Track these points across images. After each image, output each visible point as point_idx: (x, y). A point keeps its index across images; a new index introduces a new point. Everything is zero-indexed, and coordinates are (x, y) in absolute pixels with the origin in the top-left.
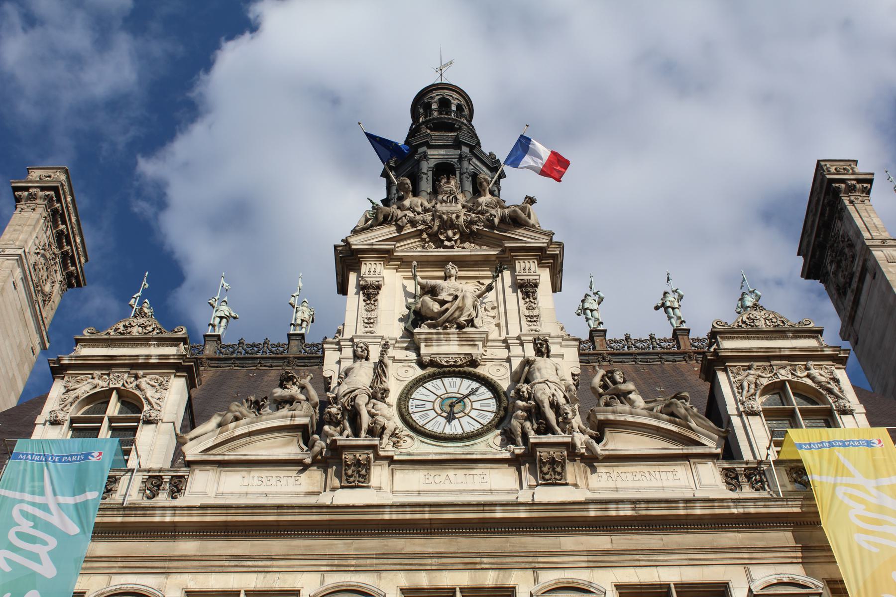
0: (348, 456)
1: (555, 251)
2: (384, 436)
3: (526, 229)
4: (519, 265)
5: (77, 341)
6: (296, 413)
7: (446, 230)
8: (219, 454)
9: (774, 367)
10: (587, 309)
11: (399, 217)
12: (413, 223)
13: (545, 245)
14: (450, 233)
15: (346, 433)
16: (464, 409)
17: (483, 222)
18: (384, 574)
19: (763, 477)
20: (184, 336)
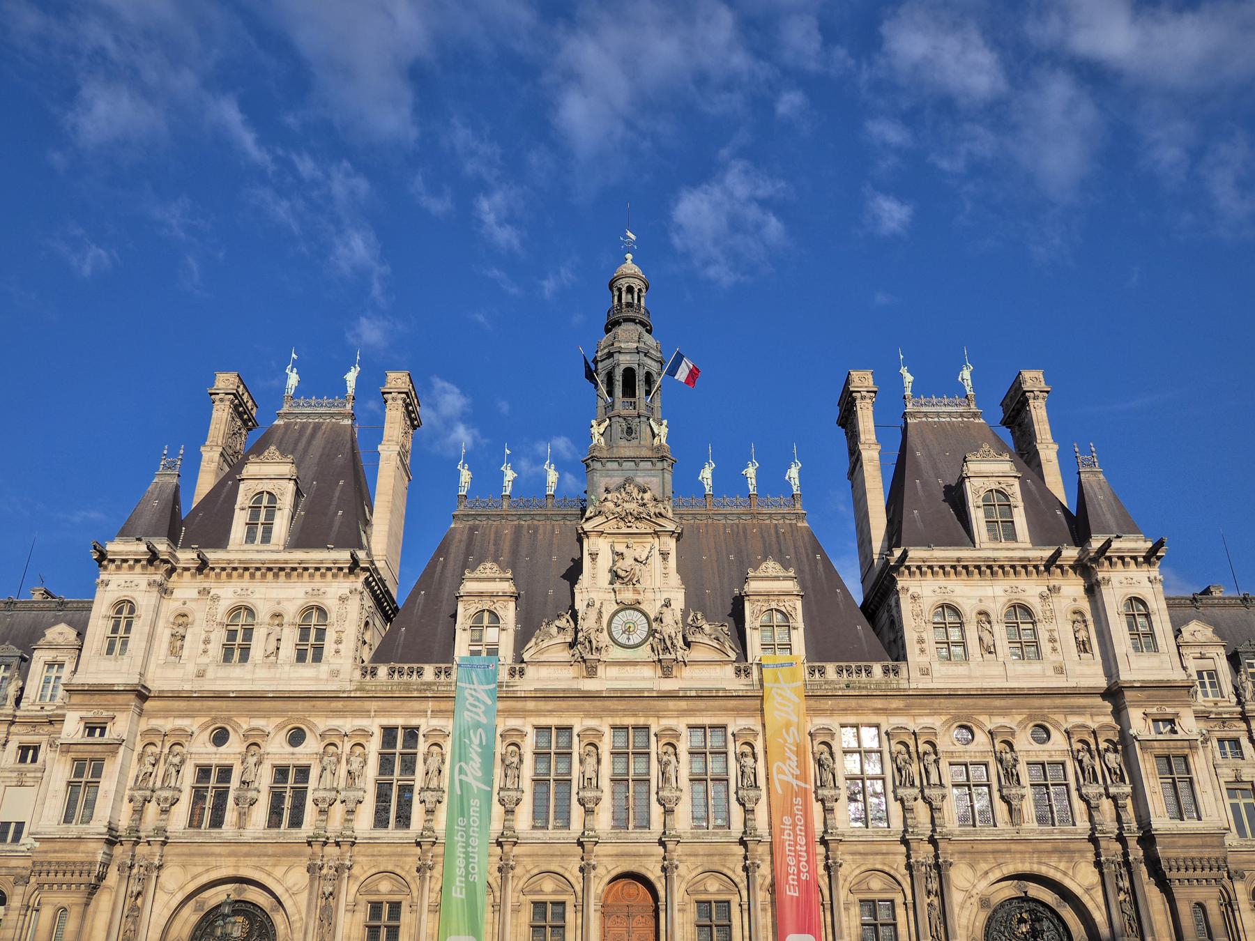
4: (662, 539)
12: (613, 514)
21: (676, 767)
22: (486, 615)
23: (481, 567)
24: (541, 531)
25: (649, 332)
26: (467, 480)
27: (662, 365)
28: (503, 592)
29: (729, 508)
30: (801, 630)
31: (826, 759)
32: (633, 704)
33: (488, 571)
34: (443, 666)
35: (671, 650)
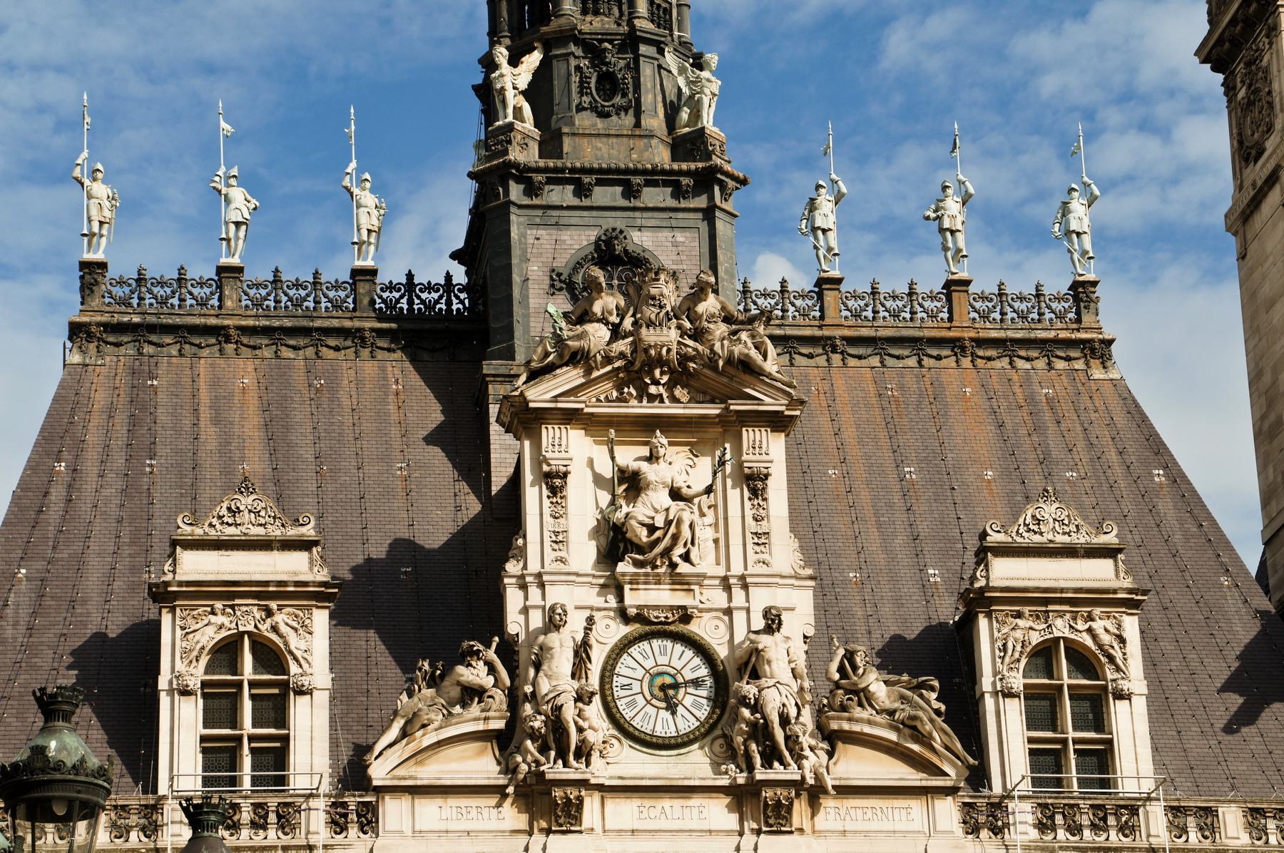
1: (796, 410)
2: (592, 752)
6: (491, 714)
9: (1051, 614)
10: (819, 228)
11: (592, 354)
13: (783, 408)
20: (316, 539)
26: (107, 213)
28: (297, 584)
30: (1140, 704)
35: (786, 753)
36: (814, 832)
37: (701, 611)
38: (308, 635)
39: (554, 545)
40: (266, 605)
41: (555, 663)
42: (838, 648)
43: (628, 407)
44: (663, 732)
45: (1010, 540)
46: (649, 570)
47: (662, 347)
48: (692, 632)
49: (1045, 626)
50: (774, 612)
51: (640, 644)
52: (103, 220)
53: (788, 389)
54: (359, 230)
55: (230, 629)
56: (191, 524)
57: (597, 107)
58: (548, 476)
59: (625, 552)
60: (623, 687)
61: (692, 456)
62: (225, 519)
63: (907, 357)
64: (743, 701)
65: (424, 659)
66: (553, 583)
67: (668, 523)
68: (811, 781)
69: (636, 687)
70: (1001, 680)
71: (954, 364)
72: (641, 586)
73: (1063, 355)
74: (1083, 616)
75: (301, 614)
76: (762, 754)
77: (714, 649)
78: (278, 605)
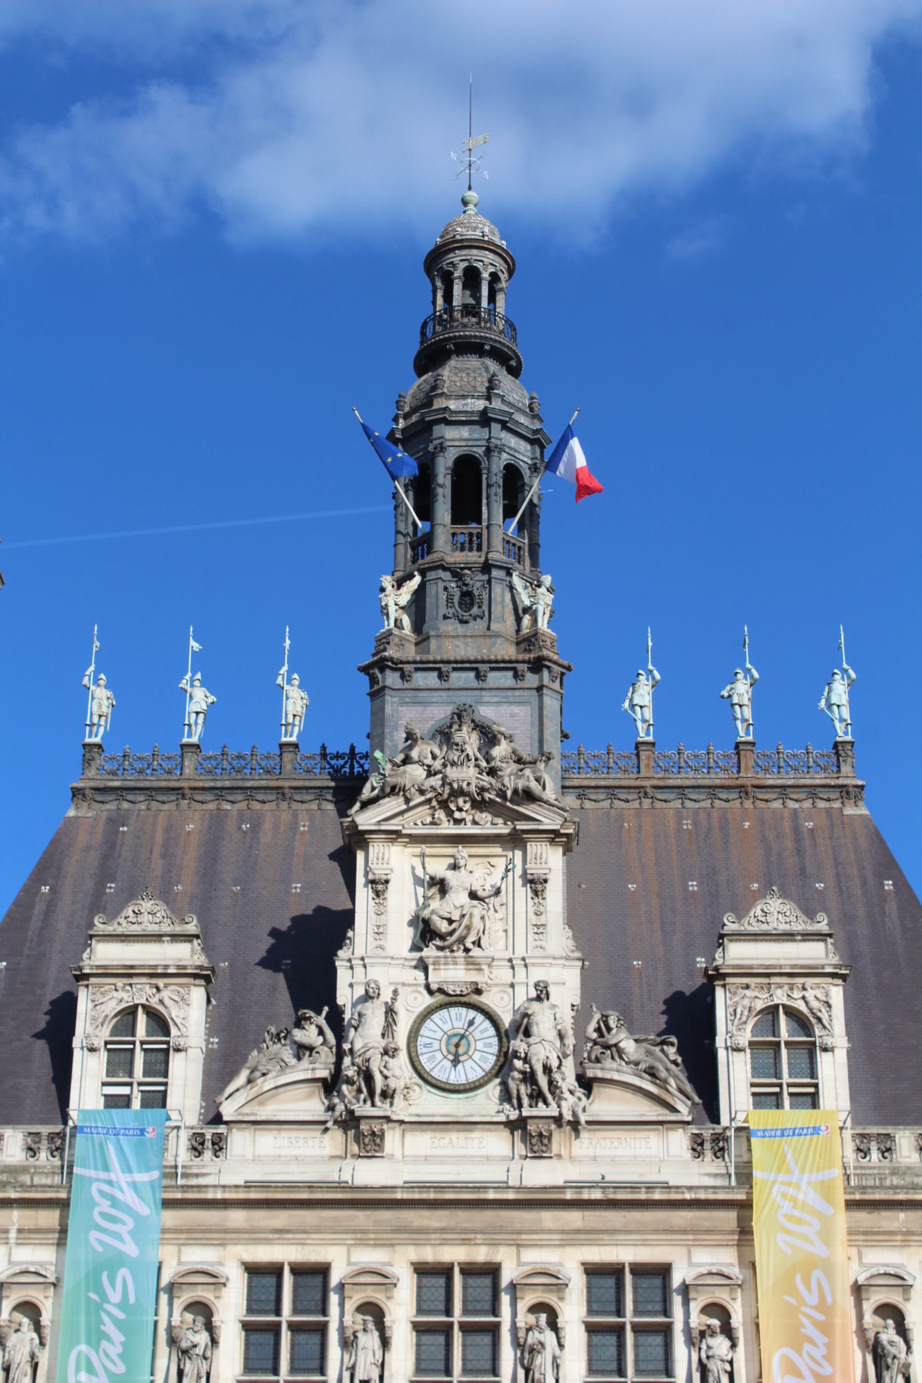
0: (364, 1127)
2: (395, 1095)
3: (539, 805)
4: (532, 848)
5: (91, 937)
6: (317, 1065)
7: (456, 797)
8: (253, 1114)
9: (772, 986)
10: (636, 705)
12: (422, 792)
13: (558, 827)
14: (460, 801)
15: (362, 1096)
16: (468, 1050)
17: (495, 790)
18: (397, 1248)
19: (726, 1144)
21: (555, 1358)
22: (142, 1019)
23: (129, 911)
24: (267, 825)
25: (515, 372)
26: (105, 710)
27: (542, 447)
29: (691, 774)
30: (840, 1057)
31: (891, 1343)
32: (463, 1217)
33: (145, 918)
34: (45, 1130)
35: (549, 1096)
36: (571, 1158)
37: (490, 986)
38: (186, 1007)
39: (376, 935)
40: (156, 984)
41: (367, 1027)
42: (595, 1013)
43: (437, 829)
44: (456, 1080)
45: (742, 928)
46: (448, 954)
47: (463, 781)
48: (482, 1002)
49: (768, 995)
50: (541, 984)
51: (441, 1012)
52: (101, 714)
53: (562, 812)
54: (286, 715)
55: (128, 1002)
56: (104, 923)
57: (458, 616)
58: (373, 882)
59: (431, 940)
60: (425, 1045)
61: (489, 866)
62: (130, 920)
63: (703, 800)
64: (516, 1055)
65: (272, 1025)
66: (373, 965)
67: (463, 916)
68: (571, 1118)
69: (436, 1045)
70: (731, 1037)
71: (738, 805)
72: (442, 967)
73: (825, 797)
74: (798, 987)
75: (181, 990)
76: (531, 1097)
77: (499, 1016)
78: (165, 984)
